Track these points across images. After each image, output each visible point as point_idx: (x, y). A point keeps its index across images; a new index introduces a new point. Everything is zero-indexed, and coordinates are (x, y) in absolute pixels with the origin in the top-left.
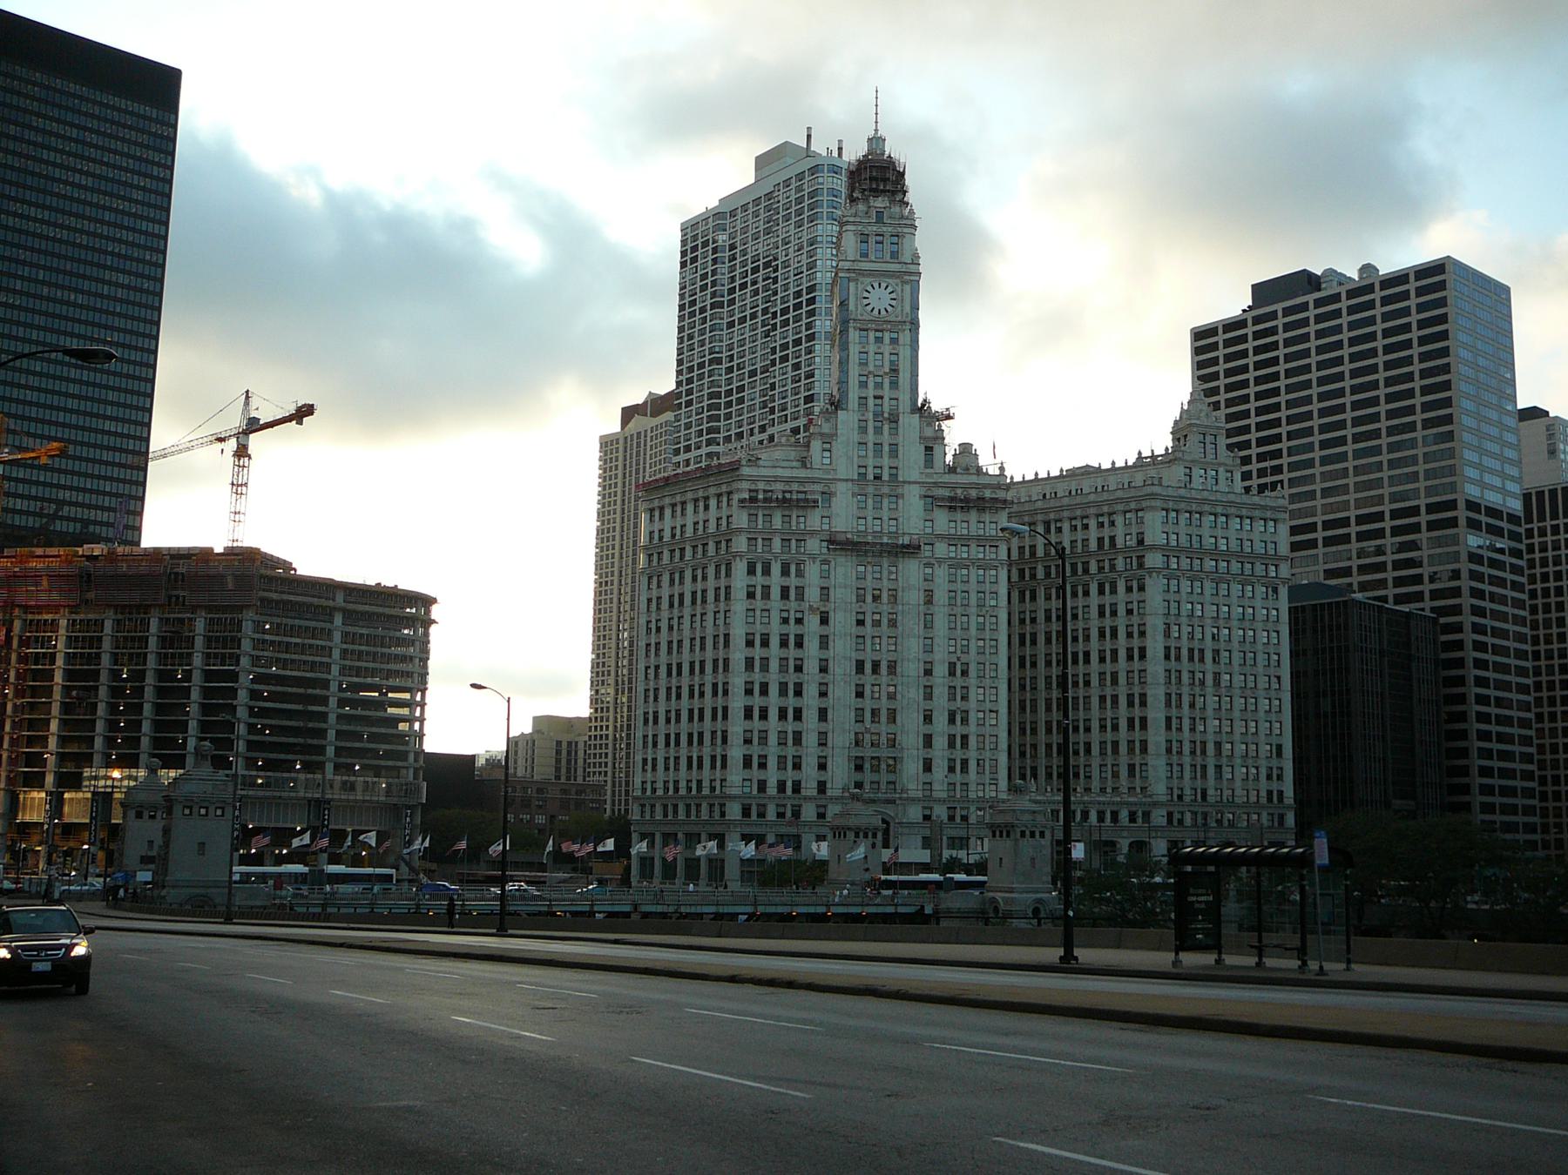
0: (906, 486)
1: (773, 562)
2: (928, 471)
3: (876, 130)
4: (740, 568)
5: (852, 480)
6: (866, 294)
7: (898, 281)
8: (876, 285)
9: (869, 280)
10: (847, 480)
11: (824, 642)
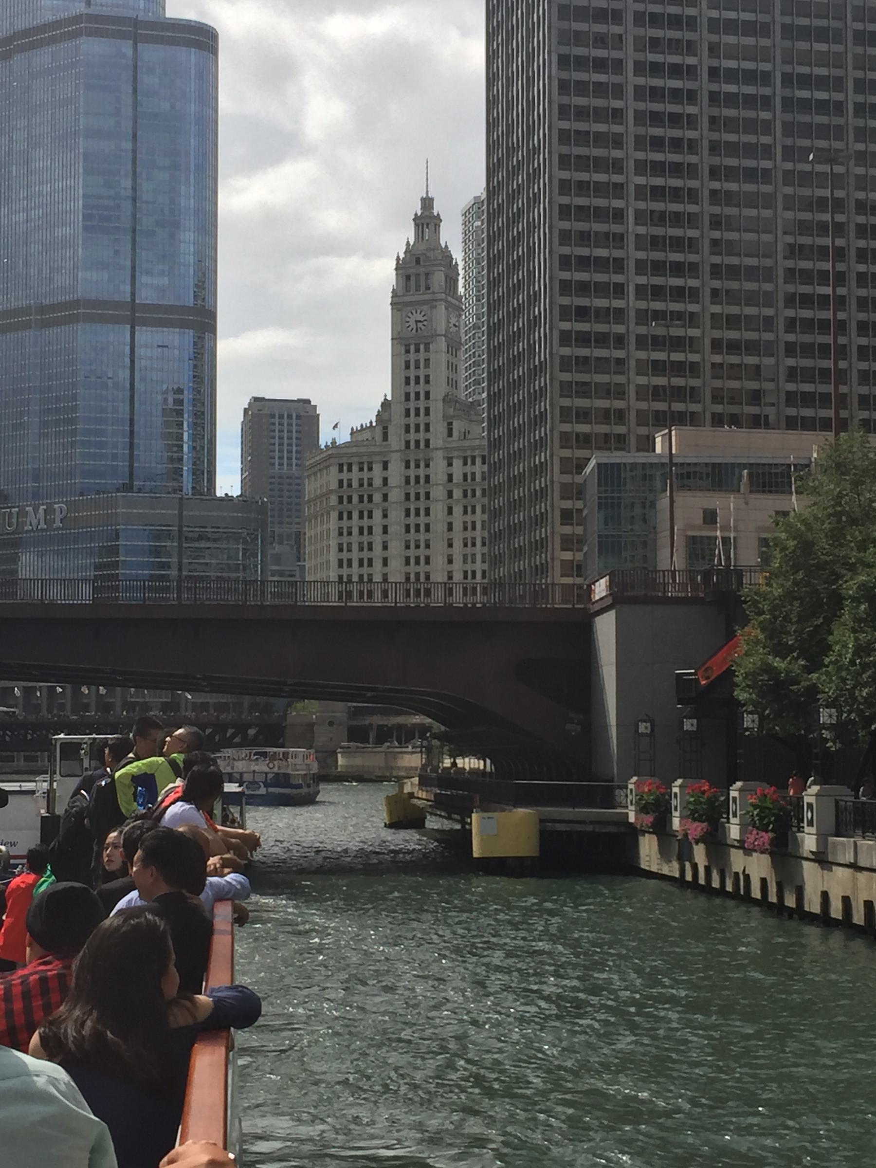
2: (450, 439)
4: (334, 515)
5: (401, 450)
6: (408, 319)
8: (414, 312)
9: (409, 308)
10: (396, 451)
11: (385, 562)
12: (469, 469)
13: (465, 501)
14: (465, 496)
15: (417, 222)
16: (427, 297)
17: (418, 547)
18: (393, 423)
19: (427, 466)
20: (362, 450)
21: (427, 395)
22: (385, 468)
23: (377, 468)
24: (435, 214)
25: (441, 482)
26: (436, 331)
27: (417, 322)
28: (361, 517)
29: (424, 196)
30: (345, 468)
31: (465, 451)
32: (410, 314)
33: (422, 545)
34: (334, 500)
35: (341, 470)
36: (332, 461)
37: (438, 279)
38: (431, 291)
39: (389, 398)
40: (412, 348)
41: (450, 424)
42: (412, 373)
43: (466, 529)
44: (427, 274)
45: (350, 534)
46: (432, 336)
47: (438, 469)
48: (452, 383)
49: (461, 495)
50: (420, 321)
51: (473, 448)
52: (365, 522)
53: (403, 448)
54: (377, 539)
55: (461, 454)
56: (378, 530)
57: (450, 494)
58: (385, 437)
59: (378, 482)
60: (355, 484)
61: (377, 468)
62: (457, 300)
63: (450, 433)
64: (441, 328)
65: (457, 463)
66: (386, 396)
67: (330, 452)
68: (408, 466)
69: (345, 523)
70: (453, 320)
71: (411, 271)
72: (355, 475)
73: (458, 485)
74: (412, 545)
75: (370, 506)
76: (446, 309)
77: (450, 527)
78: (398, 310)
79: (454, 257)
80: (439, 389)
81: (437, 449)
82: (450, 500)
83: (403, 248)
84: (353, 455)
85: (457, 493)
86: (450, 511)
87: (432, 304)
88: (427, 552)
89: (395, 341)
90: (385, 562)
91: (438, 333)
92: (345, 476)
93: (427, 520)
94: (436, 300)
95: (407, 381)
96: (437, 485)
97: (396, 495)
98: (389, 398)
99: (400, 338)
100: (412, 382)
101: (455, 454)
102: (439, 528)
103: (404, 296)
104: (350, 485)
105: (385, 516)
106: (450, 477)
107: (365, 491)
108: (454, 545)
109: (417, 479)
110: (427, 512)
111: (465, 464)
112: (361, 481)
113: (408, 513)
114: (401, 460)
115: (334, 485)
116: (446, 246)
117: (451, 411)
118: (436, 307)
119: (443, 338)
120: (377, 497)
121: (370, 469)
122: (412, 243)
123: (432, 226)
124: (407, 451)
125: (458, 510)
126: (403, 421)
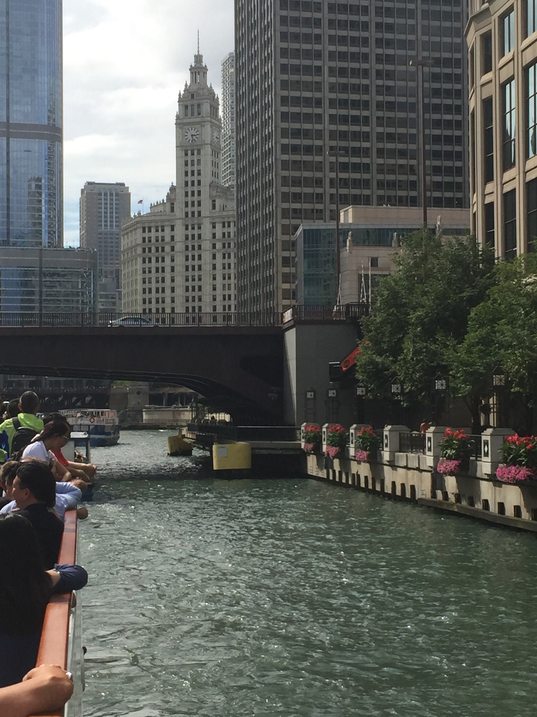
1: (152, 258)
2: (214, 211)
3: (198, 51)
4: (140, 260)
6: (186, 134)
7: (199, 126)
8: (190, 129)
9: (186, 127)
10: (180, 219)
12: (226, 230)
13: (223, 251)
14: (224, 247)
15: (192, 71)
16: (198, 120)
17: (193, 280)
18: (177, 201)
19: (199, 228)
20: (157, 218)
21: (199, 182)
22: (173, 229)
23: (167, 230)
24: (204, 66)
25: (208, 239)
26: (204, 141)
27: (192, 135)
28: (157, 261)
29: (197, 54)
30: (147, 230)
31: (224, 218)
32: (188, 131)
33: (197, 278)
34: (139, 250)
35: (144, 231)
36: (139, 225)
37: (206, 108)
38: (201, 115)
39: (175, 184)
40: (189, 152)
41: (214, 201)
42: (189, 168)
43: (224, 268)
44: (199, 105)
45: (150, 272)
46: (202, 145)
47: (206, 230)
48: (215, 175)
49: (221, 246)
50: (194, 135)
51: (228, 217)
52: (160, 265)
53: (184, 216)
54: (168, 275)
56: (168, 269)
57: (214, 246)
58: (172, 210)
59: (168, 239)
60: (153, 240)
61: (167, 230)
62: (218, 121)
63: (214, 207)
64: (208, 141)
65: (219, 226)
66: (172, 183)
67: (137, 220)
68: (187, 229)
69: (147, 265)
70: (215, 134)
71: (189, 103)
72: (153, 234)
73: (219, 240)
74: (190, 279)
75: (163, 254)
76: (211, 127)
78: (180, 128)
79: (216, 93)
80: (206, 178)
81: (205, 217)
82: (214, 250)
83: (183, 88)
84: (152, 221)
85: (219, 246)
86: (214, 257)
87: (201, 124)
88: (200, 283)
89: (178, 148)
91: (206, 142)
92: (147, 235)
94: (205, 122)
95: (186, 174)
96: (205, 240)
97: (179, 247)
98: (175, 184)
99: (182, 146)
100: (189, 174)
101: (217, 220)
102: (207, 267)
103: (184, 118)
104: (150, 241)
105: (173, 260)
106: (214, 235)
107: (160, 244)
108: (217, 279)
109: (193, 236)
110: (200, 257)
111: (224, 226)
112: (157, 238)
113: (187, 259)
114: (183, 225)
115: (140, 241)
116: (211, 86)
117: (214, 193)
118: (204, 126)
119: (209, 146)
120: (168, 248)
121: (163, 230)
122: (189, 84)
123: (202, 74)
124: (187, 218)
125: (219, 256)
126: (184, 199)
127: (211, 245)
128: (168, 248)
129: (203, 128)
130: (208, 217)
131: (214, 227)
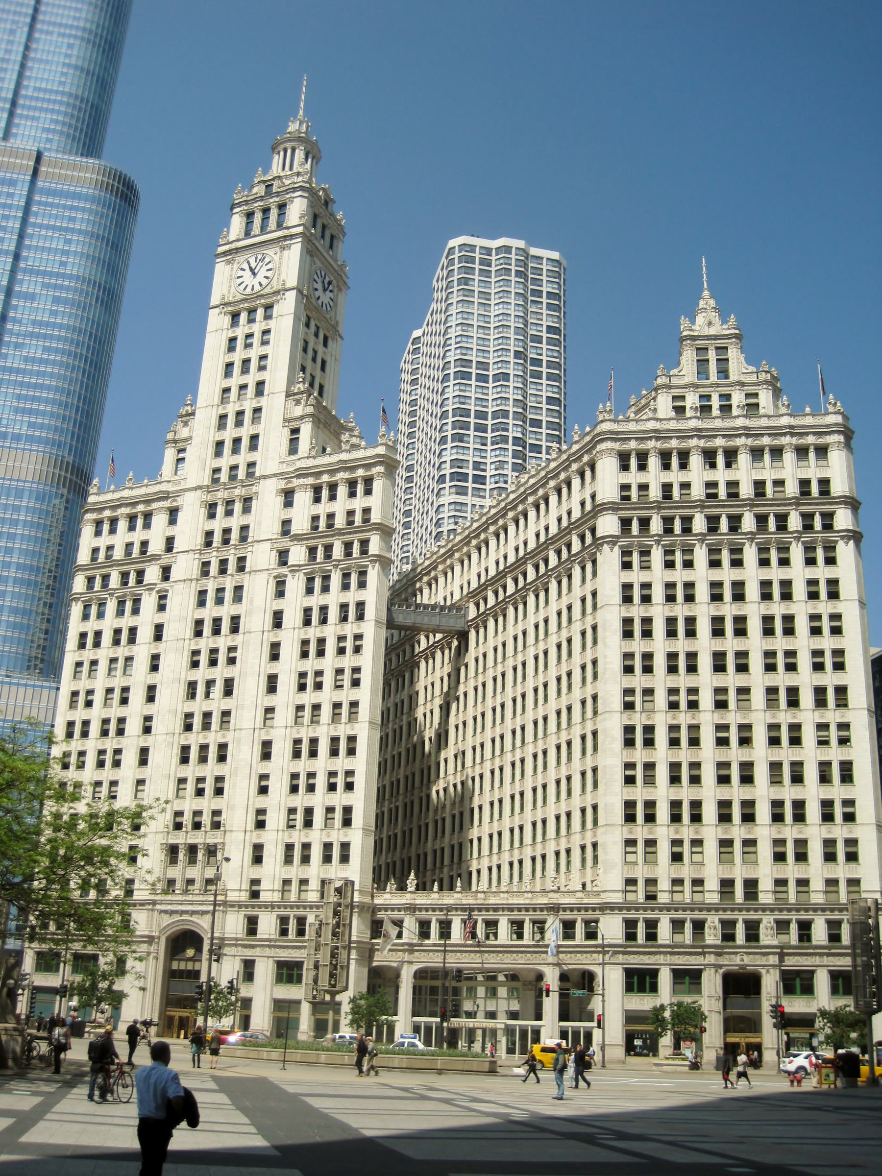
0: (262, 481)
10: (196, 489)
18: (194, 441)
22: (173, 521)
23: (160, 520)
26: (284, 284)
31: (318, 474)
41: (295, 431)
46: (277, 292)
54: (142, 651)
55: (310, 481)
57: (283, 557)
59: (156, 546)
65: (303, 498)
75: (139, 590)
77: (278, 620)
82: (284, 570)
90: (151, 695)
91: (288, 286)
93: (235, 610)
105: (162, 608)
120: (152, 574)
125: (295, 585)
127: (274, 555)
128: (152, 574)
129: (286, 252)
130: (275, 475)
131: (288, 504)
